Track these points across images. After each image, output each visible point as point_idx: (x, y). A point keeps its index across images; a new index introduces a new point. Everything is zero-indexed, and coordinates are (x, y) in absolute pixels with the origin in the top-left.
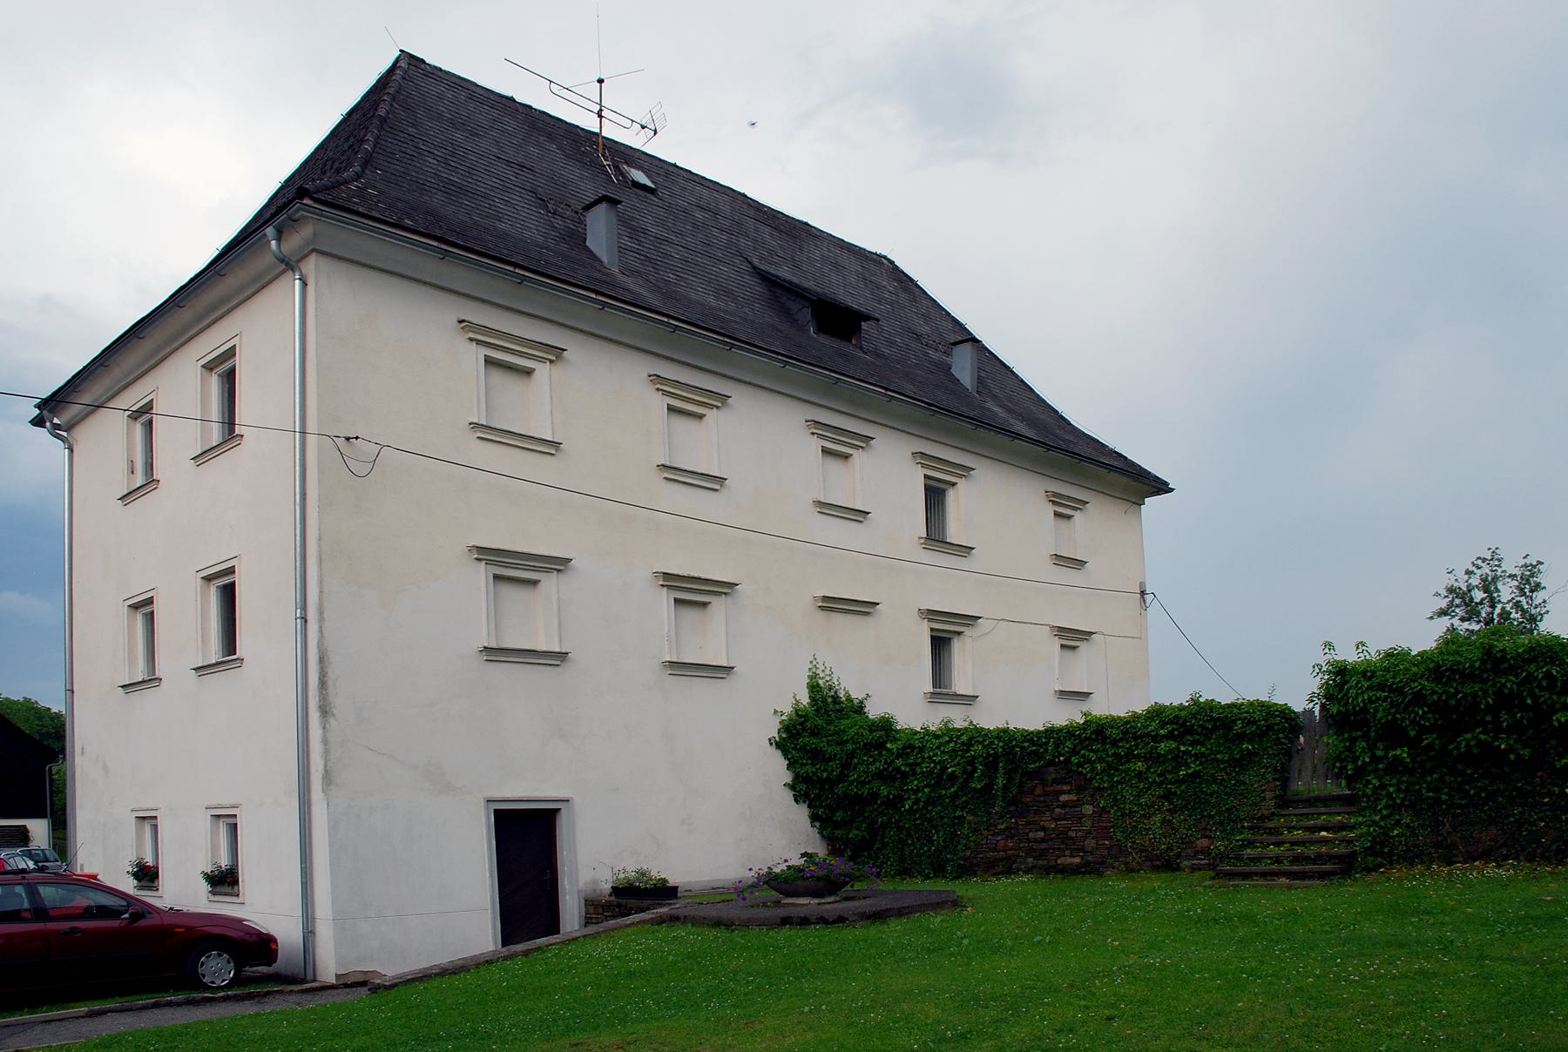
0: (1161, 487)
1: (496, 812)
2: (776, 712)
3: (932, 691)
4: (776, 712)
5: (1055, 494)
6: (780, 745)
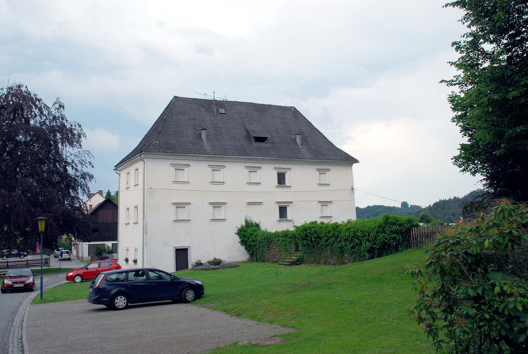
0: (356, 161)
1: (176, 249)
2: (236, 227)
3: (279, 219)
4: (236, 227)
5: (318, 169)
6: (238, 234)
